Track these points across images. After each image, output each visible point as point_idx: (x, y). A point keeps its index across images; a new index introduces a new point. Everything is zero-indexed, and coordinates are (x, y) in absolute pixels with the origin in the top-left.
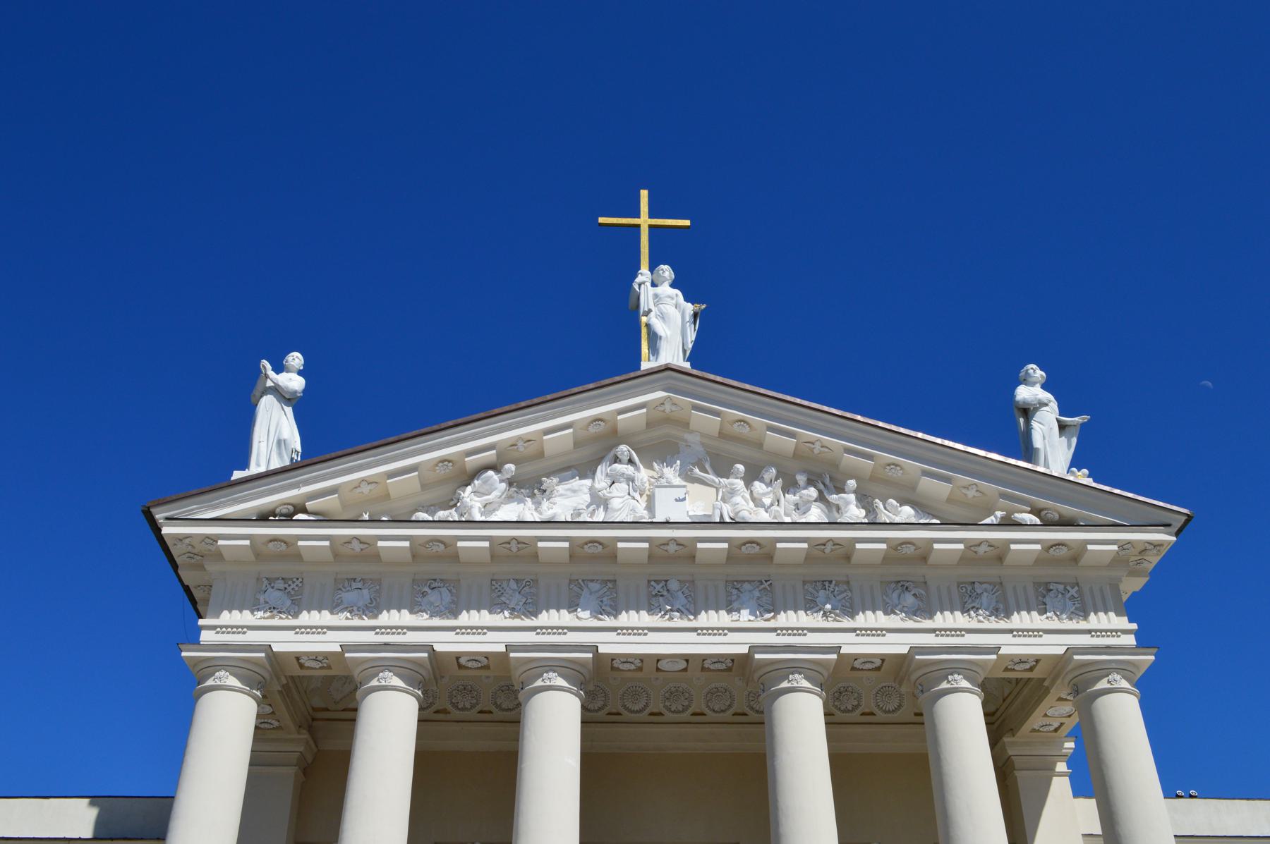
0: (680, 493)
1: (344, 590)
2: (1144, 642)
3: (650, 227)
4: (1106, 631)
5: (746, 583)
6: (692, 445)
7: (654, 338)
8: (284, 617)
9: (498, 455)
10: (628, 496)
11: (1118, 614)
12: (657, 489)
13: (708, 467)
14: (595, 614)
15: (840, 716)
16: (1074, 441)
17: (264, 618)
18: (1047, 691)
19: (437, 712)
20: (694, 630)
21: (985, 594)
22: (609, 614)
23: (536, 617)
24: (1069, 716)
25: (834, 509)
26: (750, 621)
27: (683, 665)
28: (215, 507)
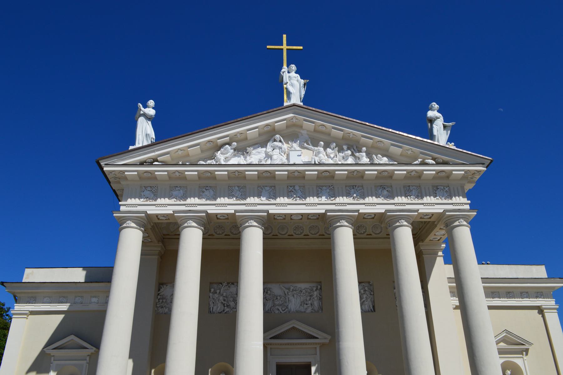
0: (299, 153)
2: (472, 208)
3: (287, 49)
4: (459, 204)
5: (324, 187)
6: (303, 135)
7: (289, 93)
8: (151, 201)
9: (230, 139)
10: (279, 154)
11: (463, 197)
12: (290, 152)
13: (310, 143)
14: (267, 198)
15: (359, 236)
16: (449, 132)
17: (144, 201)
18: (436, 226)
19: (209, 235)
20: (305, 204)
21: (414, 190)
22: (273, 199)
23: (245, 200)
24: (444, 235)
25: (357, 159)
26: (325, 201)
27: (301, 217)
28: (123, 160)
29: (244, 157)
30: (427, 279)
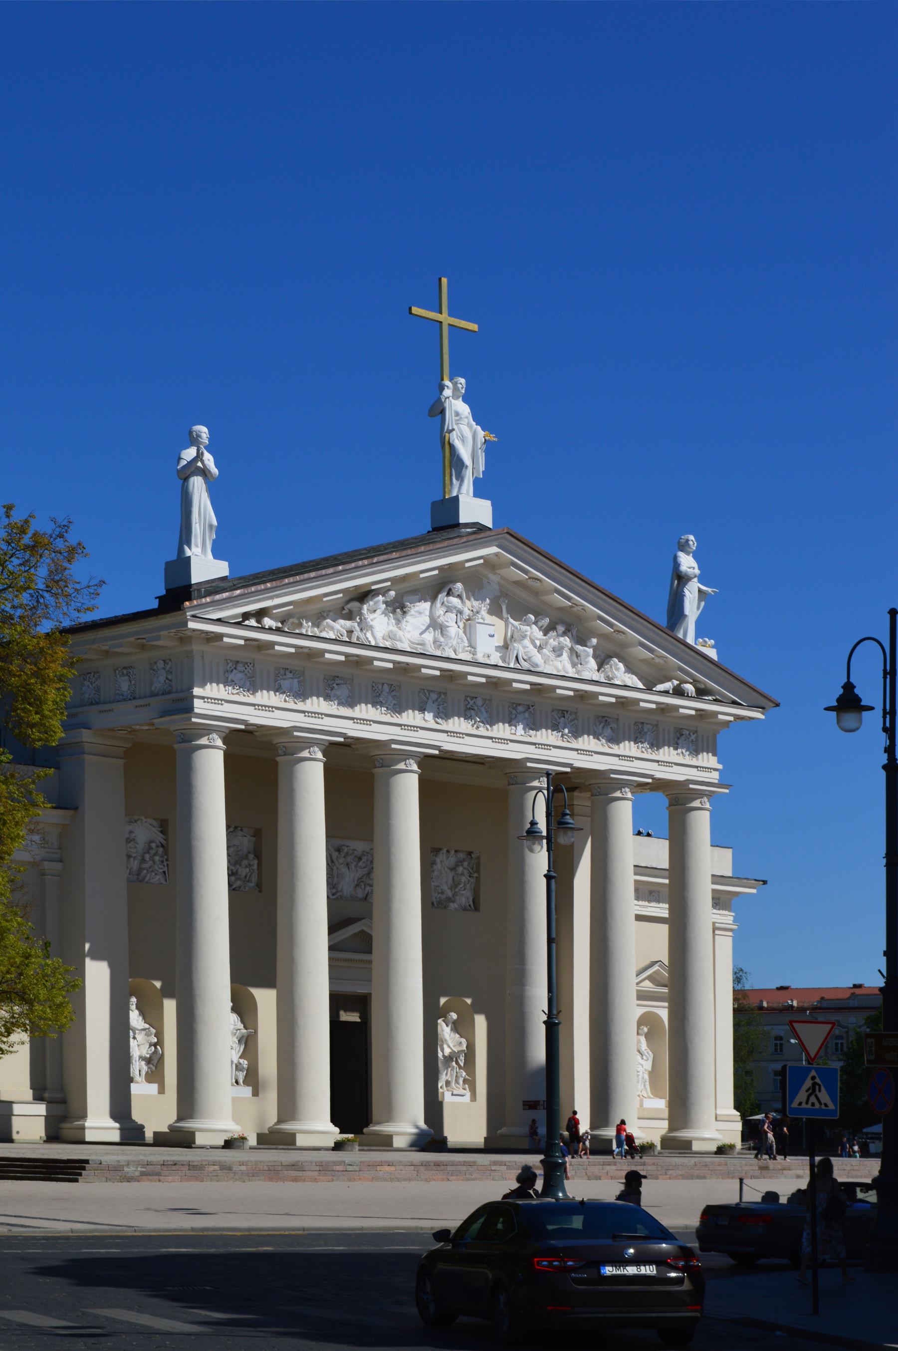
1: (281, 677)
28: (221, 609)
29: (394, 619)
30: (575, 864)
